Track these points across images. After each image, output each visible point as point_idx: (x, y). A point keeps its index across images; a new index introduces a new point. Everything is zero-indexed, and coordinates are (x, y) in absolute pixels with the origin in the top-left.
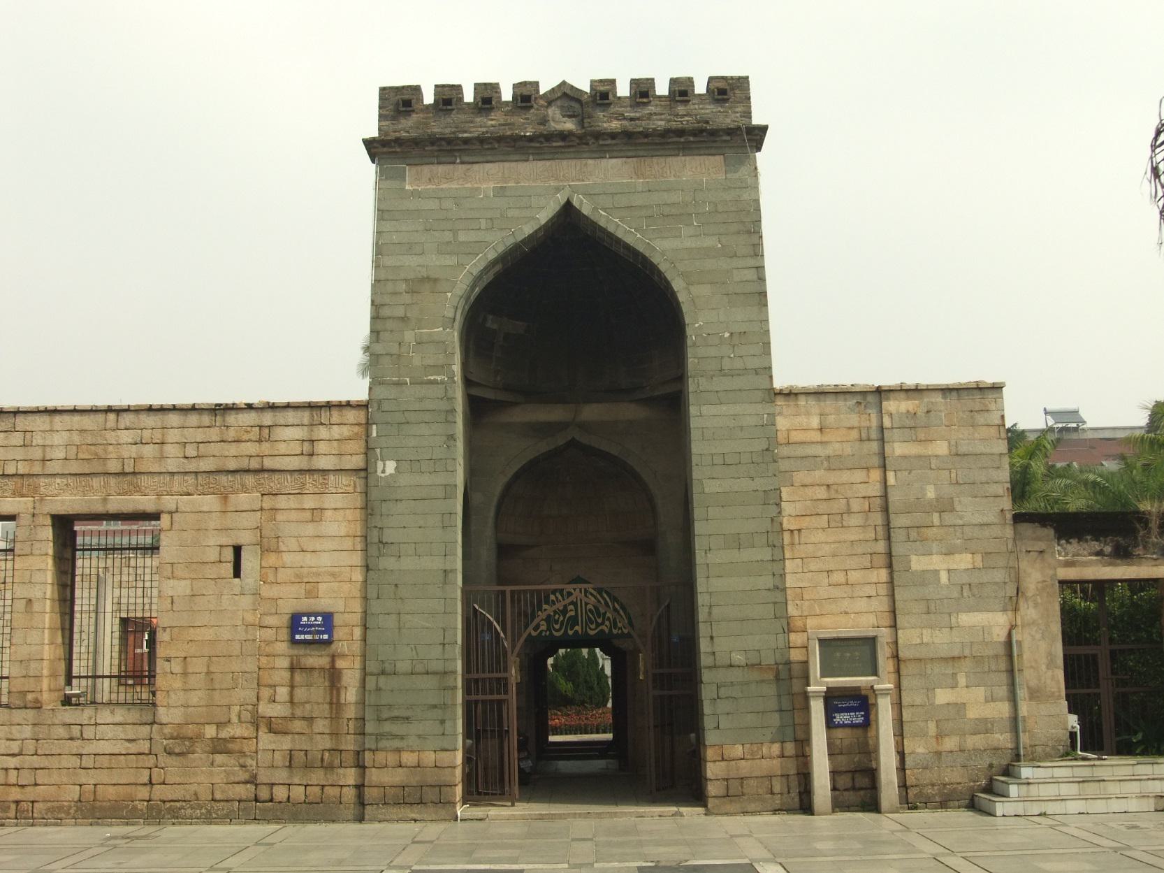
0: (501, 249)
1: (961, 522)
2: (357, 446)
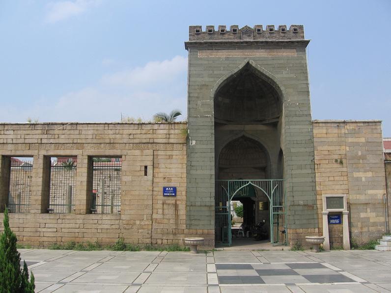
0: (228, 76)
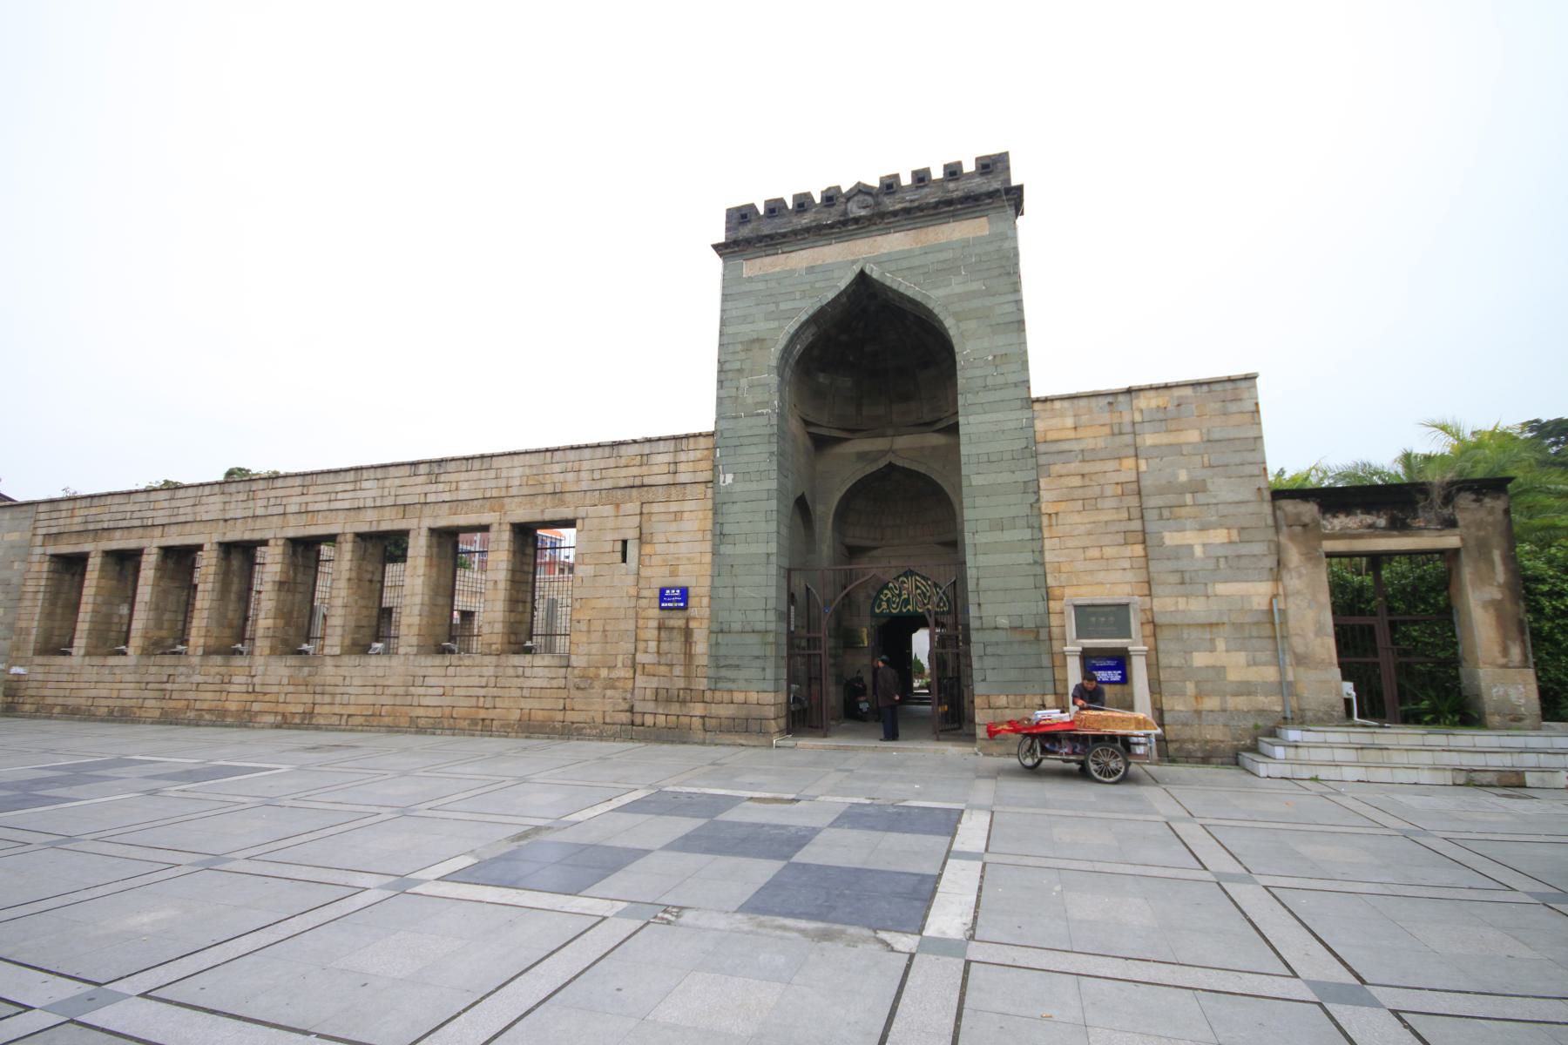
2: (706, 465)
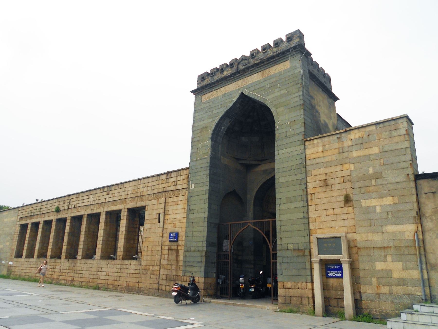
0: (223, 113)
1: (386, 183)
2: (185, 181)
